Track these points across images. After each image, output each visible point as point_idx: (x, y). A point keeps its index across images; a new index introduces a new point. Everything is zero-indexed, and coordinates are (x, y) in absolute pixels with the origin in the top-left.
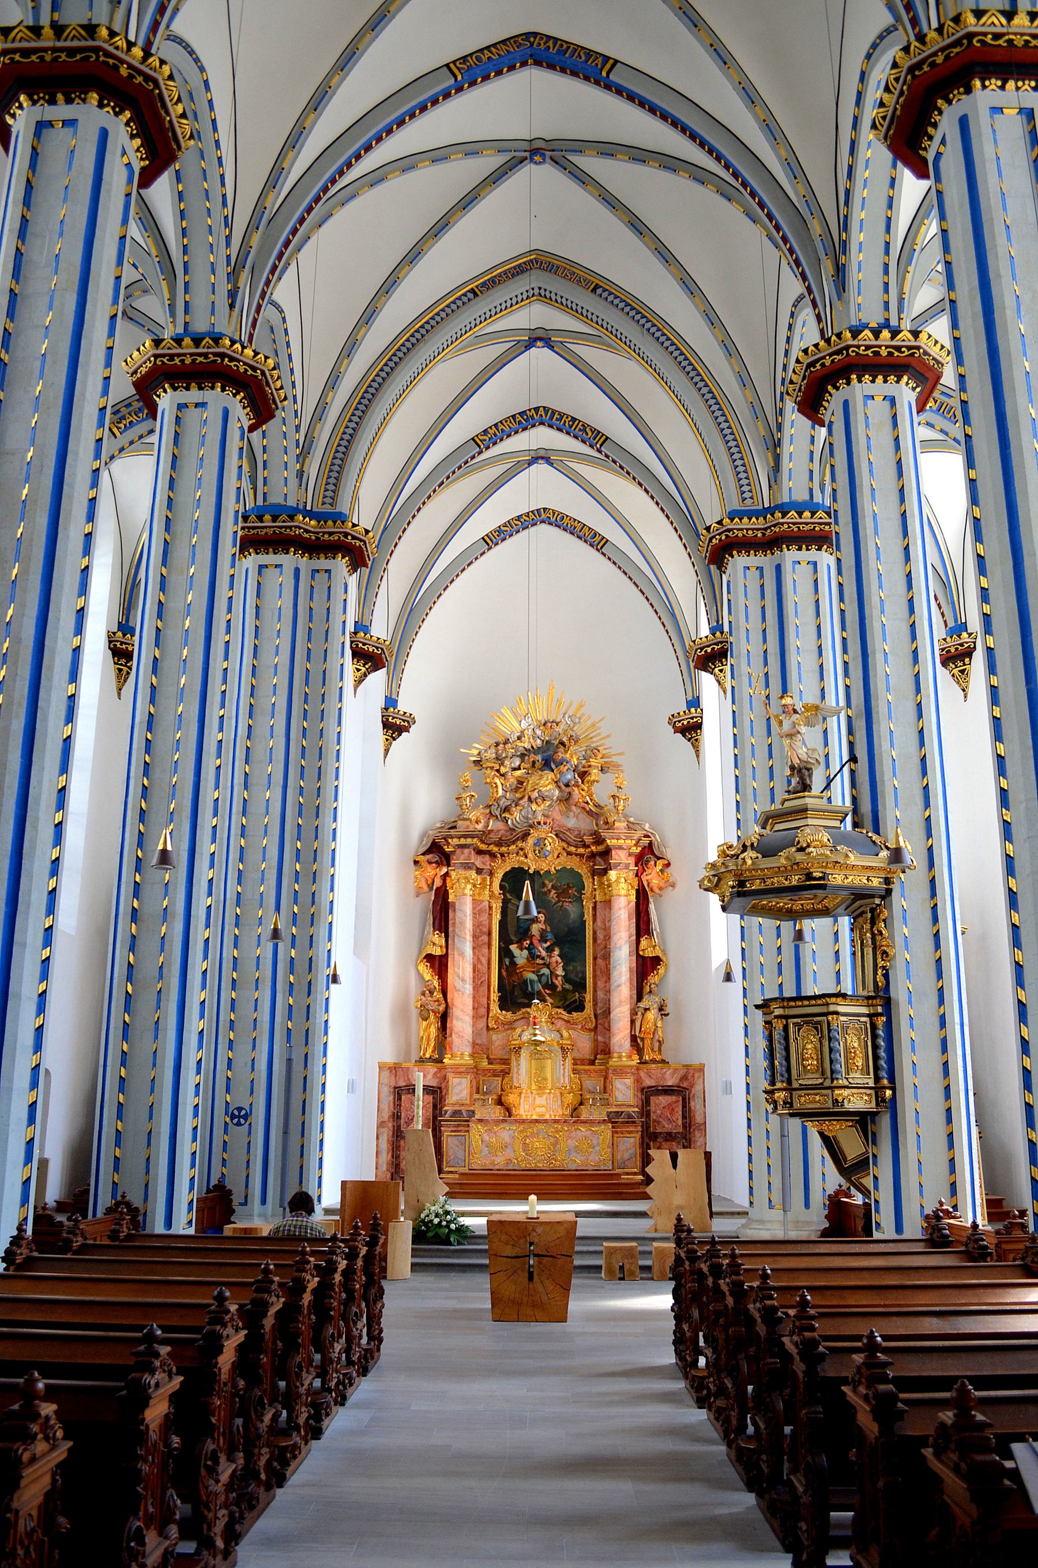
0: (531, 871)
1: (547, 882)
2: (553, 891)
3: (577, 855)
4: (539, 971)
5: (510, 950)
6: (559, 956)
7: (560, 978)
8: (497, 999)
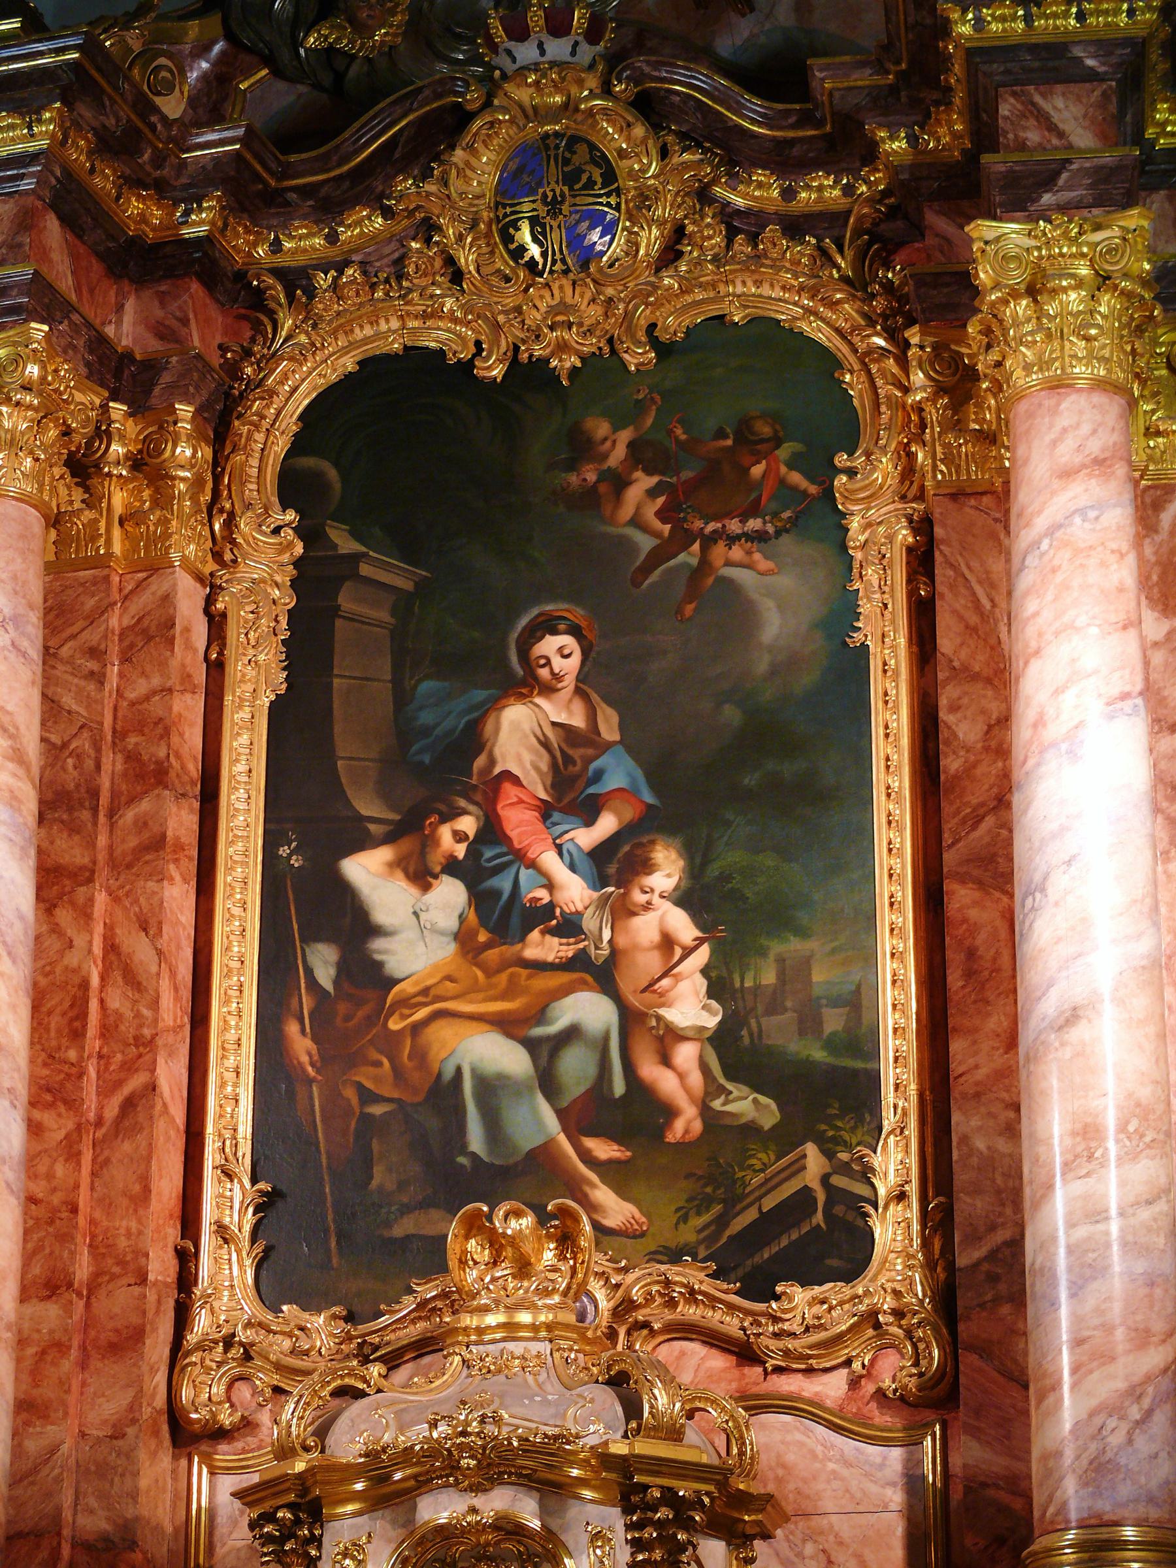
0: (494, 369)
1: (602, 428)
2: (643, 482)
3: (795, 227)
4: (540, 1015)
5: (346, 893)
6: (684, 899)
7: (686, 1054)
8: (242, 1221)
